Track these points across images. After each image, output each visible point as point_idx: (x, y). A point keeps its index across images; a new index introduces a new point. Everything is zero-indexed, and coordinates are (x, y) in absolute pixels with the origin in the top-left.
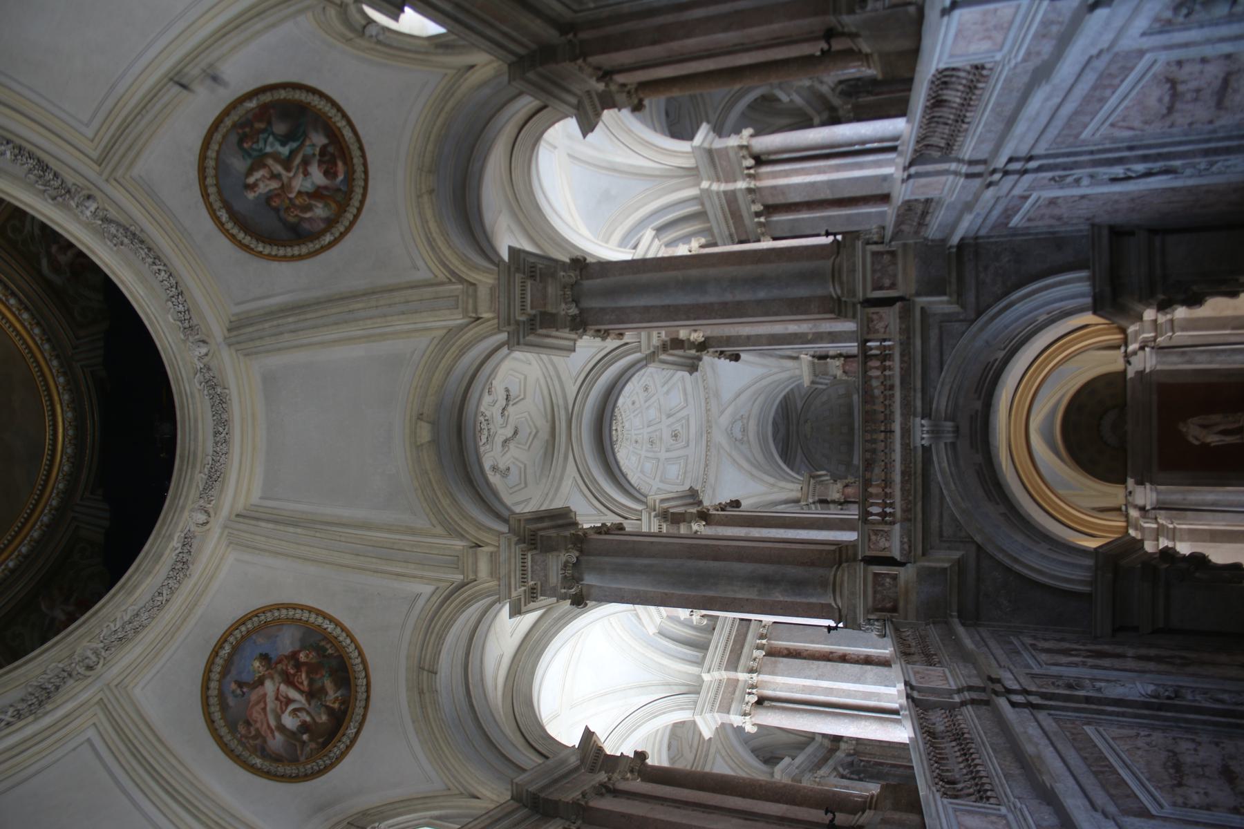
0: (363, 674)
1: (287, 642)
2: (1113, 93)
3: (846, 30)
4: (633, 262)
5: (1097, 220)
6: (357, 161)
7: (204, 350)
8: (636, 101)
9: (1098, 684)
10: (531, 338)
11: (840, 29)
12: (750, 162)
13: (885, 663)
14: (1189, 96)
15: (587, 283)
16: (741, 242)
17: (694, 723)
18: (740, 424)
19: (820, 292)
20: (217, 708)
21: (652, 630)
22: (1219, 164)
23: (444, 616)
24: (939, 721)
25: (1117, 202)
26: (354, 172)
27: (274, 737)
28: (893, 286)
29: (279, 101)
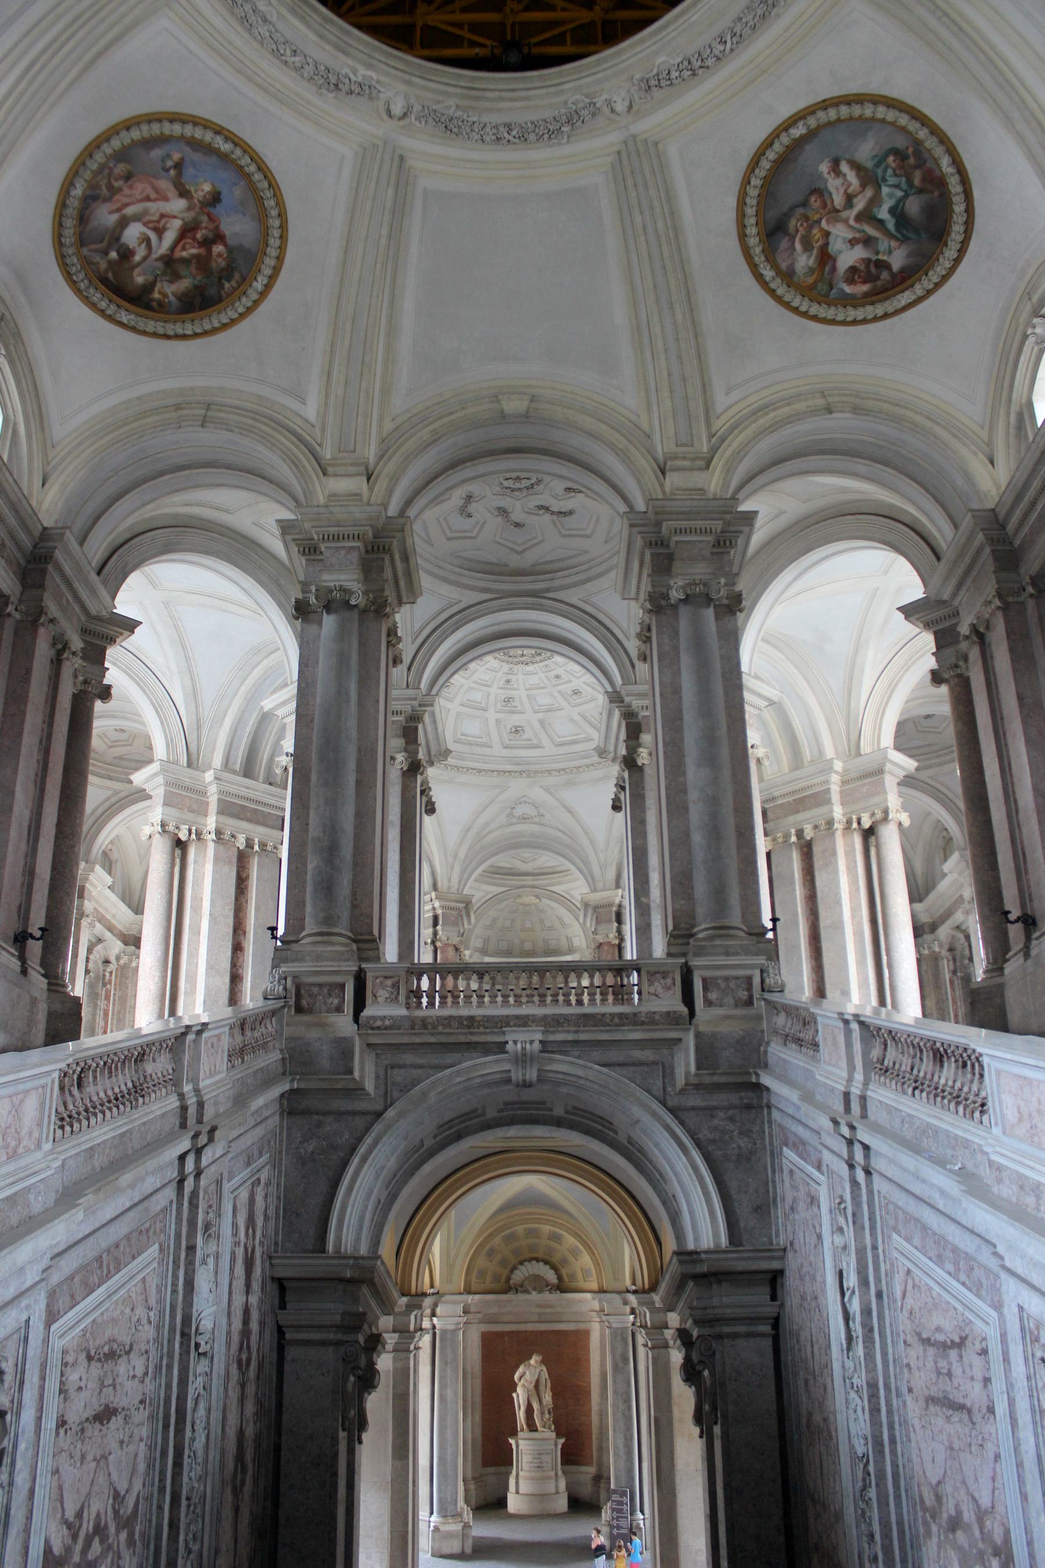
0: (198, 331)
1: (237, 227)
2: (949, 1273)
3: (1034, 943)
4: (739, 674)
5: (790, 1255)
6: (869, 311)
7: (620, 106)
8: (946, 676)
9: (211, 1261)
10: (639, 542)
11: (1036, 935)
12: (866, 824)
13: (233, 999)
14: (943, 1364)
15: (710, 613)
16: (764, 813)
17: (151, 761)
18: (530, 811)
19: (701, 911)
20: (146, 134)
21: (268, 704)
22: (858, 1401)
23: (275, 434)
24: (158, 1066)
25: (814, 1279)
26: (855, 307)
27: (111, 212)
28: (708, 1003)
29: (951, 203)
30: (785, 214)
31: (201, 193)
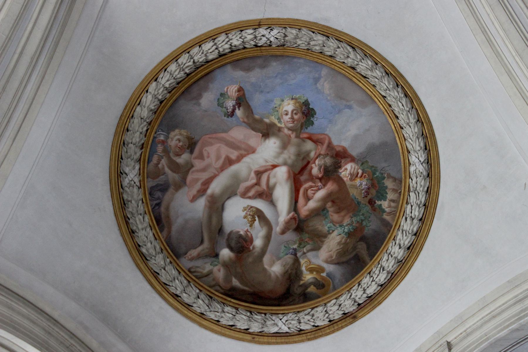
27: (194, 199)
31: (287, 118)
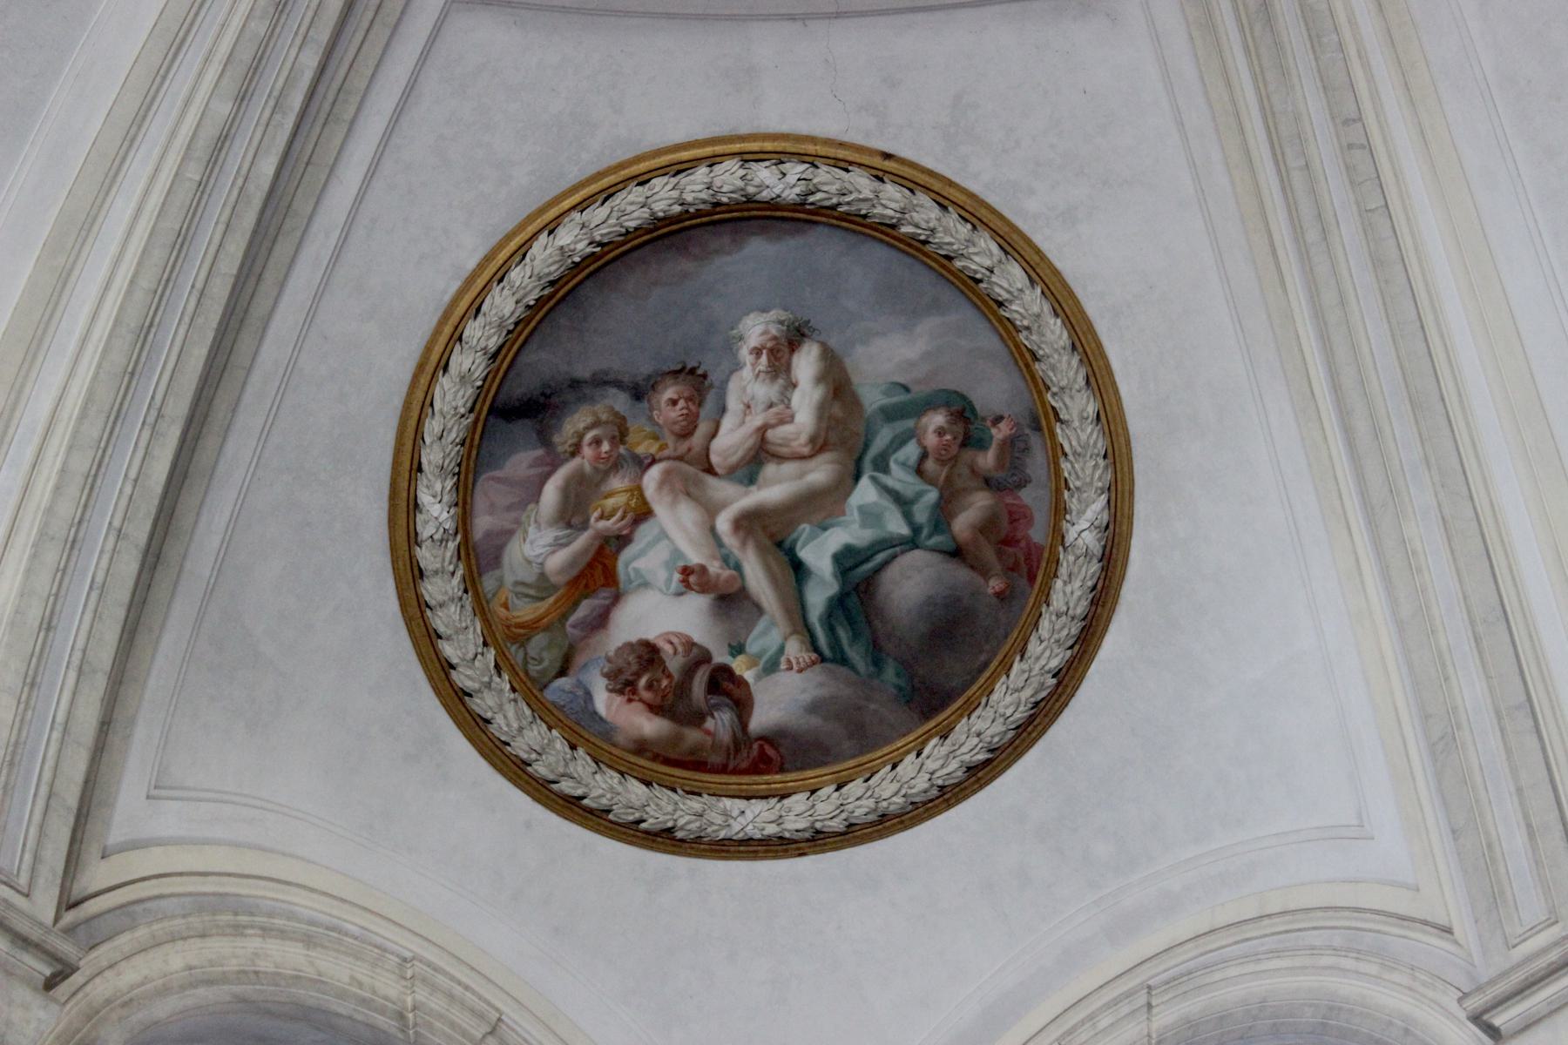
30: (575, 384)
